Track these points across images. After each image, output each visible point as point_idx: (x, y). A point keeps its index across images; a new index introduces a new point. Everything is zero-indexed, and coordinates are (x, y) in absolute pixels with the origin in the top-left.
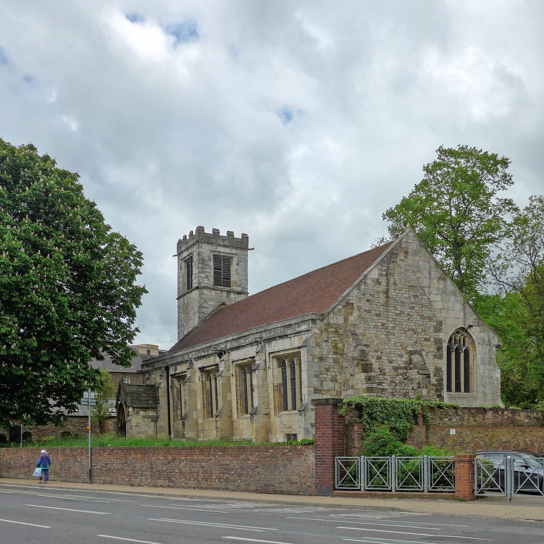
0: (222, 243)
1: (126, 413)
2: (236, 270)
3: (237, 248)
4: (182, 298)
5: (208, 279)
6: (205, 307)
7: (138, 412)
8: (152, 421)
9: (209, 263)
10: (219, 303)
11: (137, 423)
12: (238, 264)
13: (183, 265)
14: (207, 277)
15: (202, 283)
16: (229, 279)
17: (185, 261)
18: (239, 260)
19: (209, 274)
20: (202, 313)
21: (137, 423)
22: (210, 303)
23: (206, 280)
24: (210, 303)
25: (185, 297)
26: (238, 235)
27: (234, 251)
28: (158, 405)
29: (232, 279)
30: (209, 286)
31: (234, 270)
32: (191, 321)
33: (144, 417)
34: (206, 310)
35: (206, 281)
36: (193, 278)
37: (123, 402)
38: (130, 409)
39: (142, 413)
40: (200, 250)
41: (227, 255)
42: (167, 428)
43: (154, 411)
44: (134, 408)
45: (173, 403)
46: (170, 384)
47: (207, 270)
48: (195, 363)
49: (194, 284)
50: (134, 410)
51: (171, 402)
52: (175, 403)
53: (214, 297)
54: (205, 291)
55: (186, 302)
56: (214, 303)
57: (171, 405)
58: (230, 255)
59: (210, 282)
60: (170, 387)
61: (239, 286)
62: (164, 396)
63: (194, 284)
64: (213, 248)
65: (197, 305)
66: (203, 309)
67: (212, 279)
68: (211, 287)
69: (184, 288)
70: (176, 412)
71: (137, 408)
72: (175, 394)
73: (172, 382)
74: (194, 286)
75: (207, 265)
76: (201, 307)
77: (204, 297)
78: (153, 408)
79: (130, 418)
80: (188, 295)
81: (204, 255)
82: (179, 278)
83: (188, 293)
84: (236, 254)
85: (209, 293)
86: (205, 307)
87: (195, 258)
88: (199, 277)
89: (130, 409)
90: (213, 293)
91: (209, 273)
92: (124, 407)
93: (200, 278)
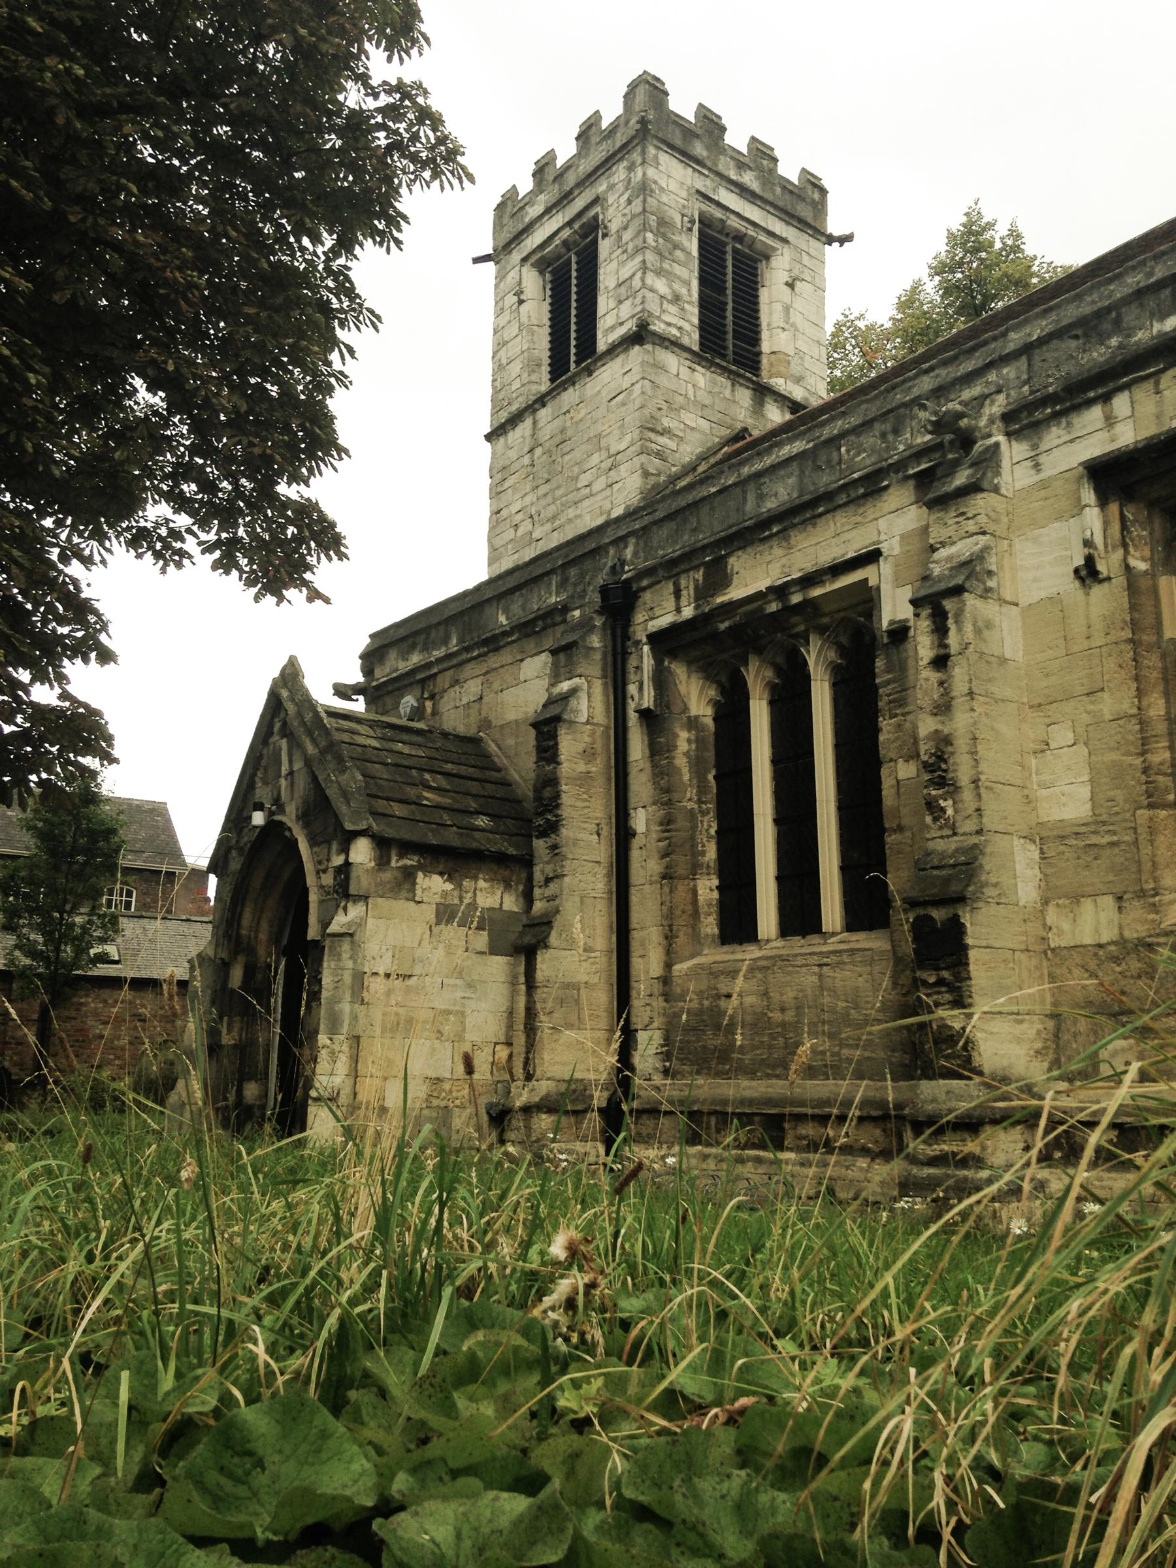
0: (734, 177)
1: (316, 884)
2: (787, 309)
3: (789, 217)
4: (525, 428)
5: (683, 309)
6: (665, 432)
7: (408, 876)
8: (494, 950)
9: (686, 244)
10: (726, 432)
11: (398, 952)
12: (791, 285)
13: (533, 283)
14: (677, 298)
15: (659, 318)
16: (755, 340)
17: (542, 266)
18: (796, 272)
19: (684, 291)
20: (659, 455)
21: (398, 952)
22: (690, 419)
23: (673, 309)
24: (690, 419)
25: (544, 414)
26: (789, 170)
27: (778, 227)
28: (540, 845)
29: (765, 347)
30: (686, 341)
31: (778, 307)
32: (586, 503)
33: (445, 914)
34: (672, 444)
35: (672, 315)
36: (604, 303)
37: (289, 817)
38: (362, 852)
39: (433, 885)
40: (651, 172)
41: (751, 232)
42: (602, 997)
43: (508, 886)
44: (382, 845)
45: (667, 823)
46: (641, 695)
47: (678, 269)
48: (1013, 452)
49: (612, 328)
50: (382, 862)
51: (640, 821)
52: (681, 823)
53: (703, 397)
54: (672, 361)
55: (545, 434)
56: (704, 425)
57: (636, 843)
58: (763, 237)
59: (687, 327)
60: (633, 718)
61: (798, 380)
62: (585, 779)
63: (612, 328)
64: (701, 184)
65: (633, 419)
66: (662, 440)
67: (693, 312)
68: (696, 348)
69: (534, 377)
70: (682, 888)
71: (407, 848)
72: (681, 762)
73: (661, 681)
74: (602, 345)
75: (676, 246)
76: (651, 427)
77: (663, 380)
78: (499, 860)
79: (355, 911)
80: (569, 396)
81: (665, 199)
82: (500, 345)
83: (563, 387)
84: (785, 241)
85: (685, 372)
86: (665, 432)
87: (615, 214)
88: (644, 286)
89: (362, 852)
90: (702, 377)
91: (687, 283)
92: (303, 846)
93: (649, 295)
